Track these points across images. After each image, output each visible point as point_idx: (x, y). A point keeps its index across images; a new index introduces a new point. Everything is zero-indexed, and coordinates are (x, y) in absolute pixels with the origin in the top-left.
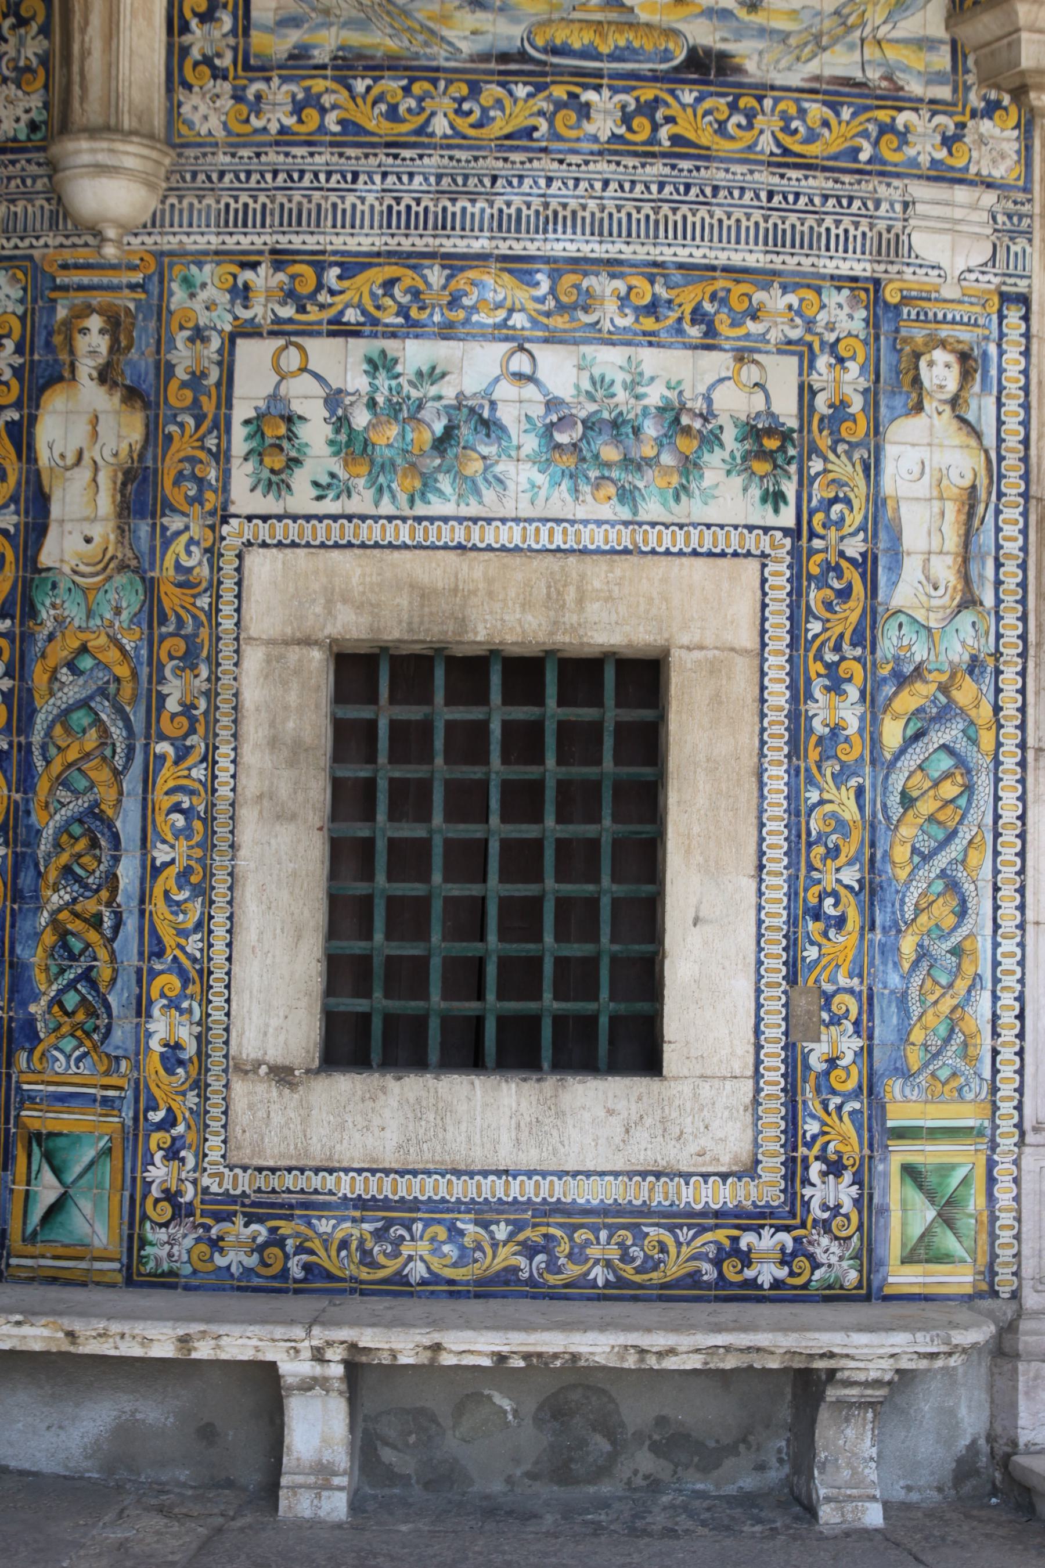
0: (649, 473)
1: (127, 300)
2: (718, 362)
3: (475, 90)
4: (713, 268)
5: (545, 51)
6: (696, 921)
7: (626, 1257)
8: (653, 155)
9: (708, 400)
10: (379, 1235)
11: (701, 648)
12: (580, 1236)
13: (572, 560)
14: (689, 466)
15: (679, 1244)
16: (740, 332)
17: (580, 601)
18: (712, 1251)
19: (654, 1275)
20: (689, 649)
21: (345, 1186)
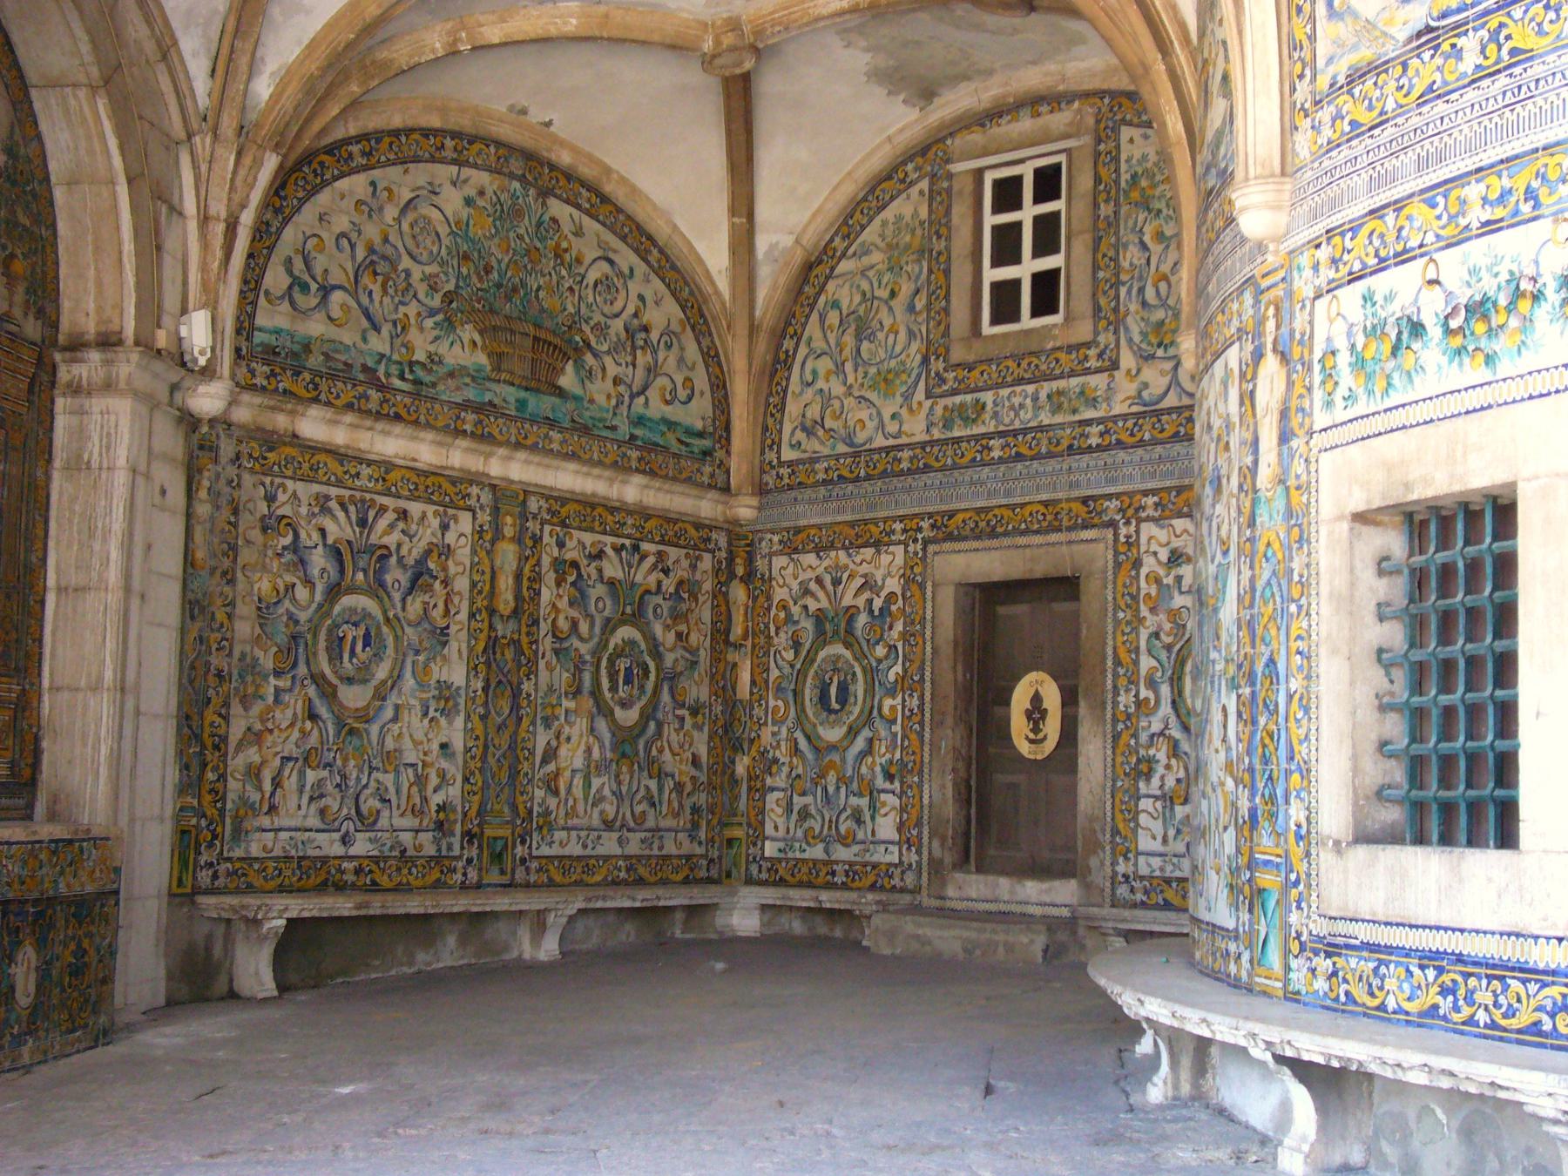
0: (1502, 337)
1: (1279, 292)
2: (1543, 227)
3: (1405, 65)
4: (1537, 150)
5: (1439, 19)
6: (1538, 714)
7: (1496, 1005)
8: (1499, 71)
9: (1537, 262)
10: (1376, 970)
11: (1537, 477)
12: (1472, 982)
13: (1460, 420)
14: (1527, 321)
15: (1528, 996)
16: (1554, 198)
17: (1465, 454)
18: (1549, 1004)
19: (1513, 1021)
20: (1529, 480)
21: (1364, 933)
